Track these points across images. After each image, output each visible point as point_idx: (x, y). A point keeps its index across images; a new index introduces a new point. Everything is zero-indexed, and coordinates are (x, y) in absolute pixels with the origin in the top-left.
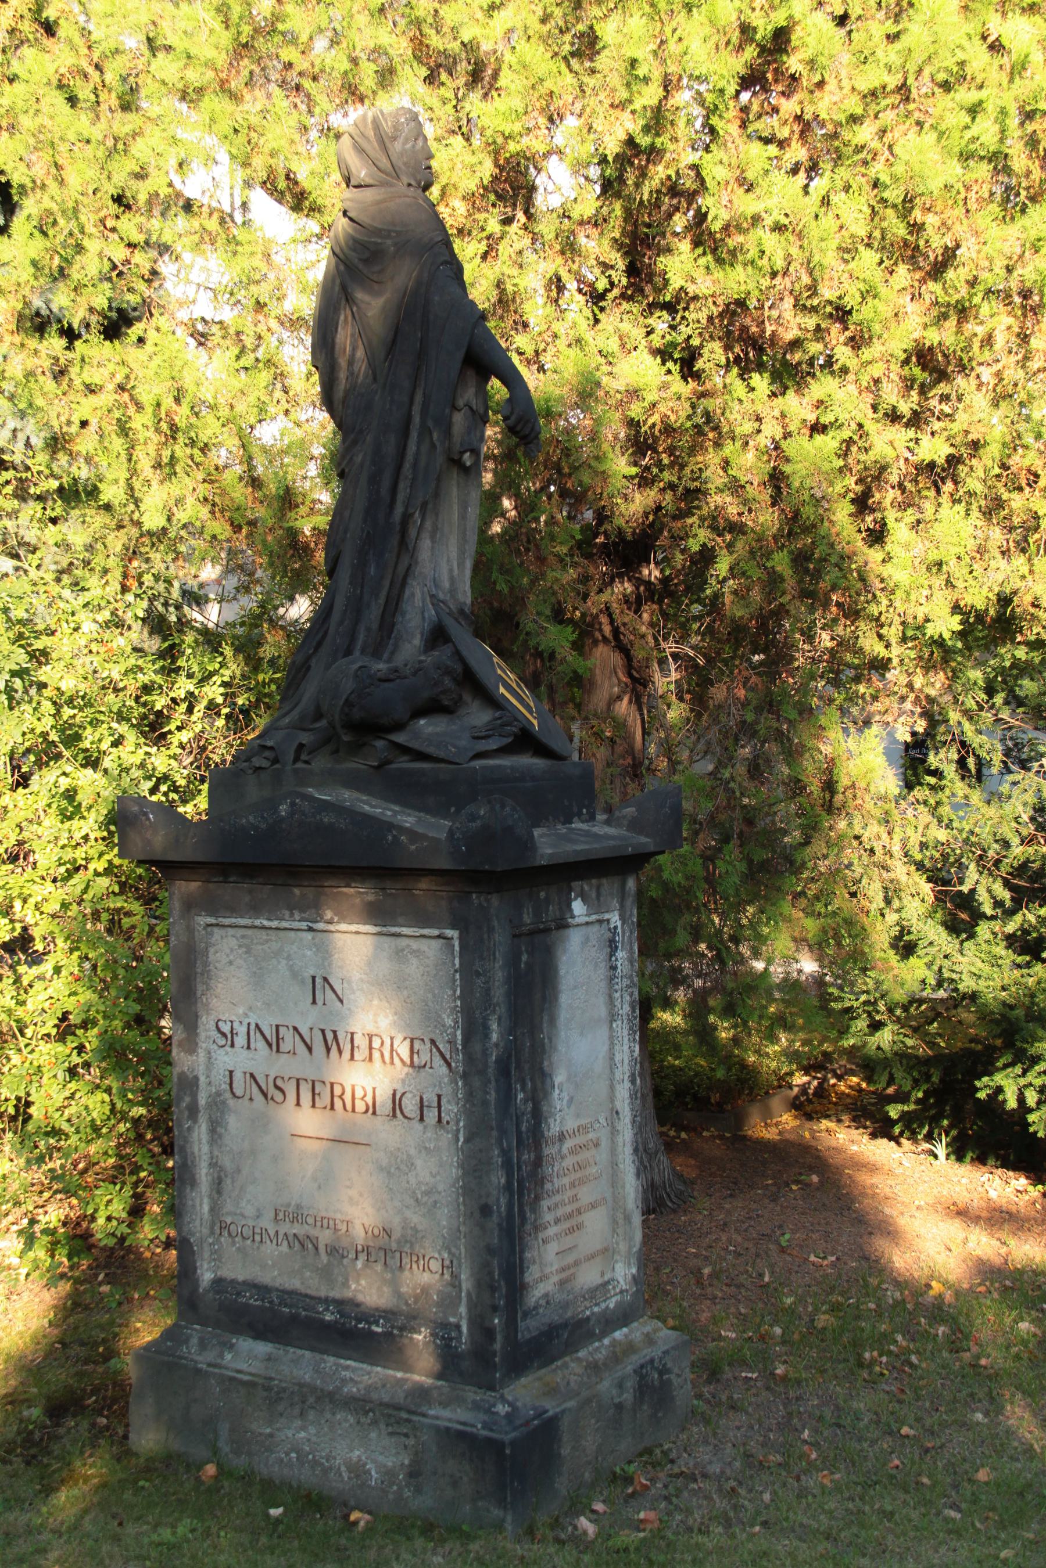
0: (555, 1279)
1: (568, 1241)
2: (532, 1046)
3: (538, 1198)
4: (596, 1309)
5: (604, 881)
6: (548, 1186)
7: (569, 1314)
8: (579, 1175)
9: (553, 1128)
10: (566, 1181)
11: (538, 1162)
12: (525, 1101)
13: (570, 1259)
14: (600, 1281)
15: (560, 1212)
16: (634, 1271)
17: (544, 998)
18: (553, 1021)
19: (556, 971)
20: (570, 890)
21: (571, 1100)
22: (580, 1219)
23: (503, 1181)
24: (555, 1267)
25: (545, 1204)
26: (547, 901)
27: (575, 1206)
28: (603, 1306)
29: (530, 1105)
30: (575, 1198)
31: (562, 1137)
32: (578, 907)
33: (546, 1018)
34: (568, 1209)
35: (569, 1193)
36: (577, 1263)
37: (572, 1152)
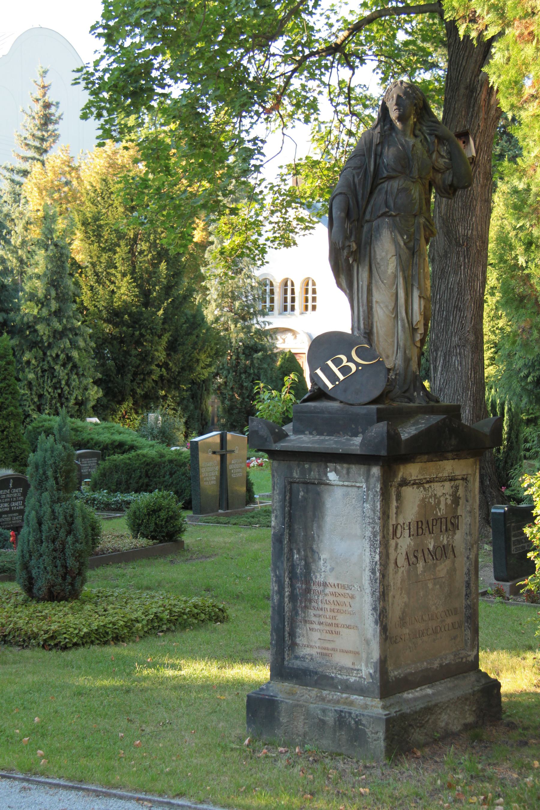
0: (319, 651)
1: (329, 637)
2: (306, 535)
3: (306, 607)
4: (339, 676)
5: (353, 466)
6: (313, 604)
7: (320, 670)
8: (337, 607)
9: (319, 578)
10: (328, 607)
11: (308, 590)
12: (300, 559)
13: (330, 646)
14: (352, 667)
15: (322, 620)
16: (371, 671)
17: (314, 515)
18: (320, 527)
19: (323, 503)
20: (327, 467)
21: (332, 569)
22: (337, 629)
23: (276, 588)
24: (317, 645)
25: (312, 612)
26: (310, 470)
27: (334, 622)
28: (345, 677)
29: (303, 563)
30: (334, 618)
31: (325, 585)
32: (332, 476)
33: (315, 525)
34: (329, 621)
35: (329, 614)
36: (333, 649)
37: (333, 594)
